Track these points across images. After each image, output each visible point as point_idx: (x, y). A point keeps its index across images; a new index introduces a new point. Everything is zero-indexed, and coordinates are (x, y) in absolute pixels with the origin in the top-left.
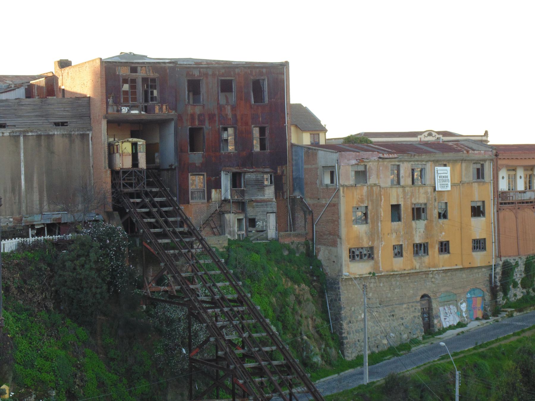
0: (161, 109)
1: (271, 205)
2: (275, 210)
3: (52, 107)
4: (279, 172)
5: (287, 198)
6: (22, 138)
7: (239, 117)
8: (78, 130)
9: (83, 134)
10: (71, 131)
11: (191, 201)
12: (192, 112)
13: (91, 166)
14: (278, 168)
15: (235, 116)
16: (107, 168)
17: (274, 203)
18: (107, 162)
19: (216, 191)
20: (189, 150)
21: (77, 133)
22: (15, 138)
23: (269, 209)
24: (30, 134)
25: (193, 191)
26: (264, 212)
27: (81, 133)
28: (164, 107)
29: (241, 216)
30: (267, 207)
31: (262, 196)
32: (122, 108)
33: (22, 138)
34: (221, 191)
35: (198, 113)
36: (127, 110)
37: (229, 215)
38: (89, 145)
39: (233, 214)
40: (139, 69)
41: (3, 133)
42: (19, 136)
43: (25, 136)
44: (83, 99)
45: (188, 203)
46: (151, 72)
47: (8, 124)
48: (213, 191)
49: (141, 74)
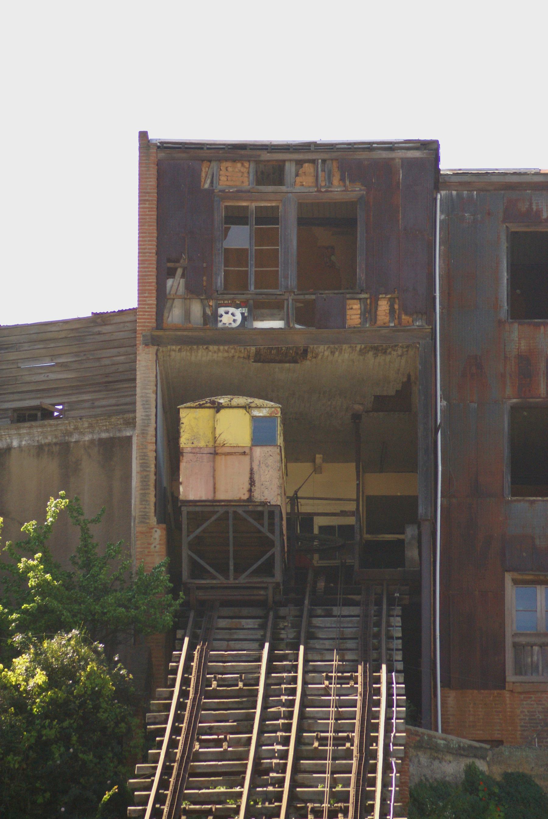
3: (12, 356)
8: (91, 426)
10: (70, 434)
11: (510, 677)
12: (523, 345)
16: (153, 520)
18: (152, 499)
20: (507, 490)
21: (87, 438)
25: (522, 640)
27: (104, 435)
28: (383, 306)
32: (221, 310)
36: (239, 318)
38: (127, 478)
40: (290, 169)
44: (118, 319)
45: (501, 683)
46: (336, 181)
49: (298, 188)
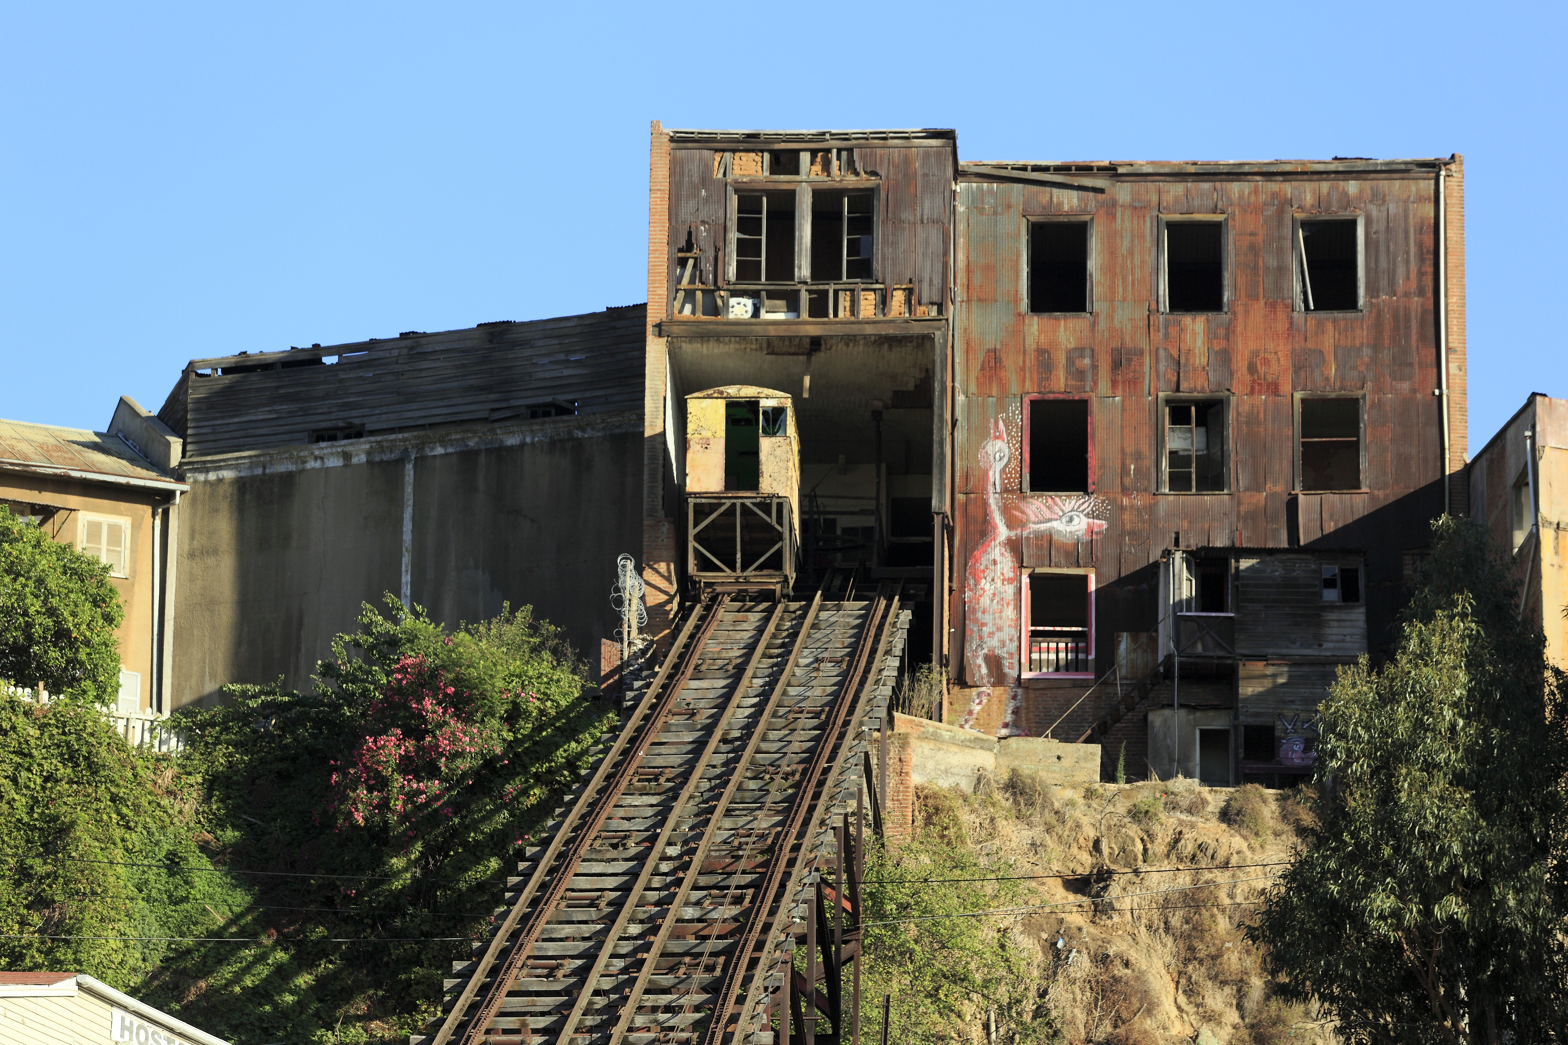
0: (884, 302)
3: (527, 352)
6: (409, 468)
7: (1240, 365)
16: (661, 513)
19: (1135, 639)
22: (386, 472)
24: (439, 451)
29: (1218, 722)
33: (409, 468)
34: (1155, 641)
37: (1167, 712)
38: (639, 474)
39: (1183, 713)
41: (347, 456)
42: (401, 461)
43: (421, 462)
47: (368, 427)
48: (1124, 644)
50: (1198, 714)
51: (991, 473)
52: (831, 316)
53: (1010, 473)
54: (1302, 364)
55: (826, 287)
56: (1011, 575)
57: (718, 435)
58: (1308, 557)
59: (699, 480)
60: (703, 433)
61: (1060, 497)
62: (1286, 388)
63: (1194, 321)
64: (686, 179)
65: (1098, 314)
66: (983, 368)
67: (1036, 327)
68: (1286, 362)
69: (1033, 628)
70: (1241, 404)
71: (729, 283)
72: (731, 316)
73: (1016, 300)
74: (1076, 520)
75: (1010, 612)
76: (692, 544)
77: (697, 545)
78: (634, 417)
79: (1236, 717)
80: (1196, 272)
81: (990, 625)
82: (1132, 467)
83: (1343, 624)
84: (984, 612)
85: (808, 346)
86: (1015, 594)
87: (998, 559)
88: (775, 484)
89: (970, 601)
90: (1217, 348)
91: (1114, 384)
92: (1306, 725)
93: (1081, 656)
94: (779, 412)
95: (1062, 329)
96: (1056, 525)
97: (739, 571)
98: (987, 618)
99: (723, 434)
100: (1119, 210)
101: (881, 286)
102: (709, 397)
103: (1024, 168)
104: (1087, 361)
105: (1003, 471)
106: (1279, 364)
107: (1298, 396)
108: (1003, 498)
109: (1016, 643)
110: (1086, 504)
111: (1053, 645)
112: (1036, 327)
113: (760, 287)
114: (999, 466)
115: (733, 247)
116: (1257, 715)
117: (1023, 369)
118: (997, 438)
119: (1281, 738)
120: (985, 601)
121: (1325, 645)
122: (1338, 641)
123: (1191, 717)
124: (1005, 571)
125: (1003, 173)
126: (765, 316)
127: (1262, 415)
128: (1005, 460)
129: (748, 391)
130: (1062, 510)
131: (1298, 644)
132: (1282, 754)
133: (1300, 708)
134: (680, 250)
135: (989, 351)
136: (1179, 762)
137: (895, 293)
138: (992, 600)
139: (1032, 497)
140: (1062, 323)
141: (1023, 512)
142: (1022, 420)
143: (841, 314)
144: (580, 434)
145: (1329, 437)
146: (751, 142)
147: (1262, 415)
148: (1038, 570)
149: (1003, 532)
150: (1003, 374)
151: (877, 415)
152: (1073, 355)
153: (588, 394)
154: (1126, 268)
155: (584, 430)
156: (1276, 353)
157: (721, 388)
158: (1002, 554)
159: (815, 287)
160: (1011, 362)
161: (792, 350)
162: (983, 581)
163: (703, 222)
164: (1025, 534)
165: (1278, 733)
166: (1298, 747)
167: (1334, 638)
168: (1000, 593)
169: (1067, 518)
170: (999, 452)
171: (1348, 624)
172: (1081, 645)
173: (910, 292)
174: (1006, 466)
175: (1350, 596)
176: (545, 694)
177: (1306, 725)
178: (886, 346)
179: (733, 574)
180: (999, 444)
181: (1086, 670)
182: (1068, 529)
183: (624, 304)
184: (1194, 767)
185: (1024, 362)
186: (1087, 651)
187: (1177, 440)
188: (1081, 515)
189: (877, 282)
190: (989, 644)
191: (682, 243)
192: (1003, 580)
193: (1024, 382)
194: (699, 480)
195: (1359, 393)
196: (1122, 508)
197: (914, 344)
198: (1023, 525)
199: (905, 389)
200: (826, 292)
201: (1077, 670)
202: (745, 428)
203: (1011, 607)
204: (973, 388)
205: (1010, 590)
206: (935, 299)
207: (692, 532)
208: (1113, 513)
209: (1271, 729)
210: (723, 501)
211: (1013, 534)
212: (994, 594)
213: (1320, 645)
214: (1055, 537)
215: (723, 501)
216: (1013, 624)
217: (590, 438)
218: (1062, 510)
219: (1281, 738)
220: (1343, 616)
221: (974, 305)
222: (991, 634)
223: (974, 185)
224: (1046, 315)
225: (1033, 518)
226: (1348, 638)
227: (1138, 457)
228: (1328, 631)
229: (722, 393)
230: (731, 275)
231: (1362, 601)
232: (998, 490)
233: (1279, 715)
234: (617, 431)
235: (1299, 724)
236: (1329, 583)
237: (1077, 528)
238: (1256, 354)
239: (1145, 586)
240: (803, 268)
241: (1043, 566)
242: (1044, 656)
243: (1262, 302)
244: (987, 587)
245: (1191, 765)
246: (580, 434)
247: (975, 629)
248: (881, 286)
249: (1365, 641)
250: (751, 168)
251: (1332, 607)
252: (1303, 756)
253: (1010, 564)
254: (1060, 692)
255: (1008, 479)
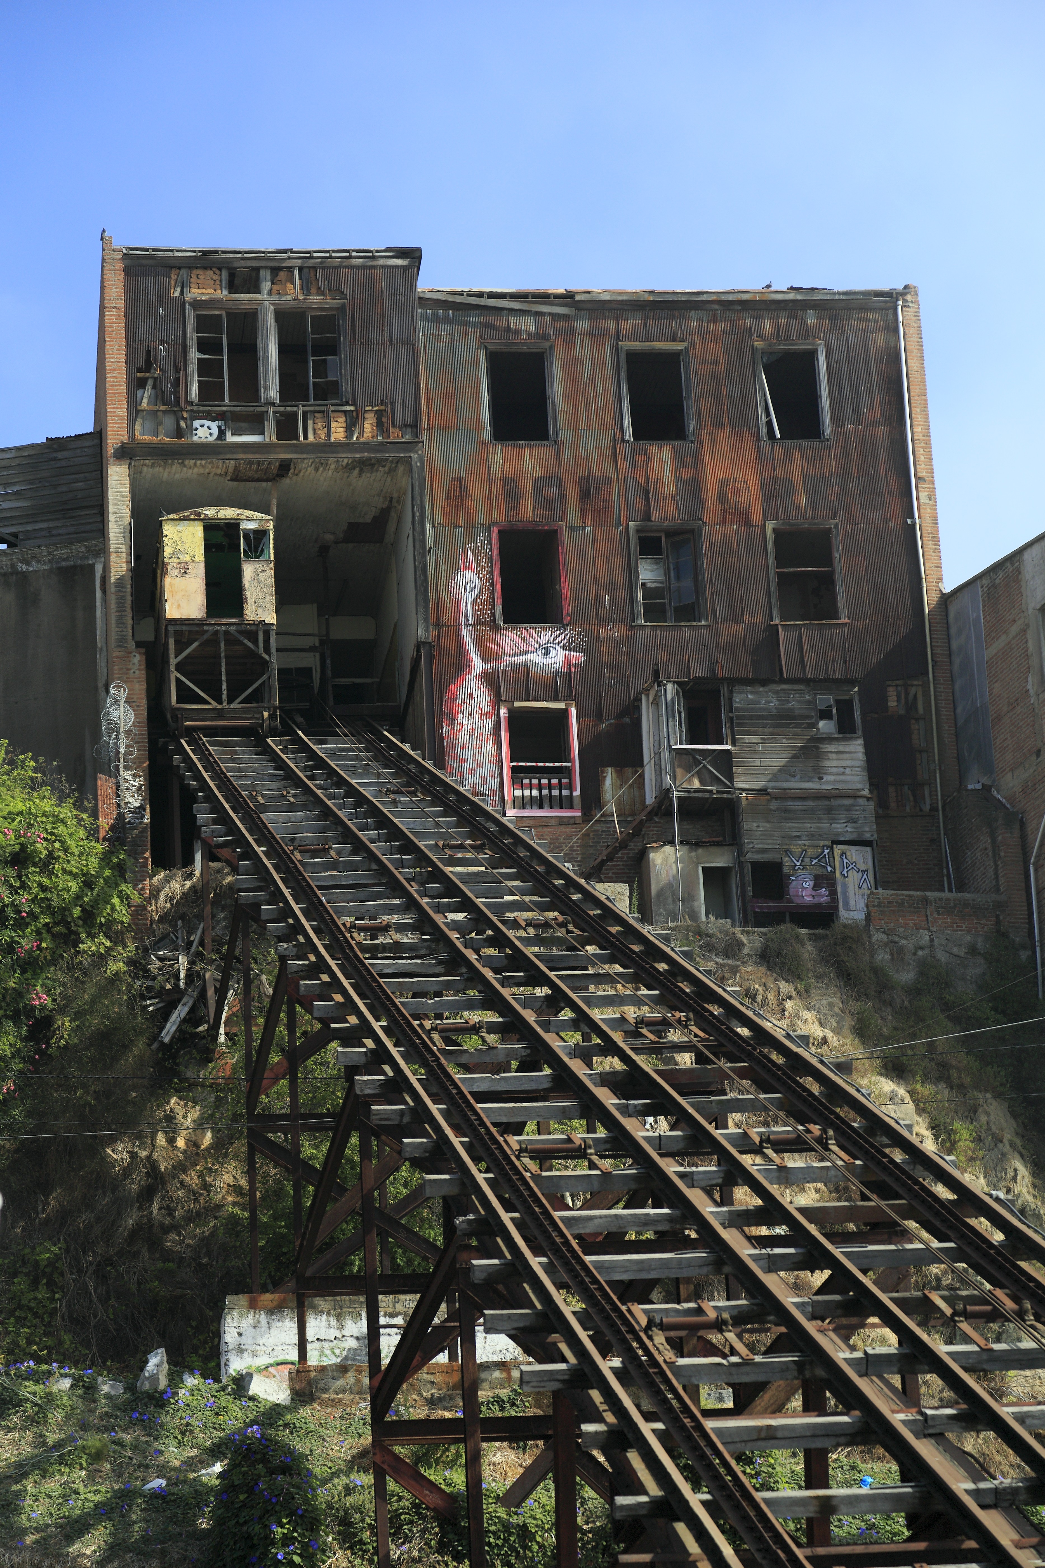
1: (848, 809)
2: (869, 831)
4: (892, 703)
5: (934, 809)
9: (74, 567)
13: (100, 684)
14: (892, 692)
15: (693, 488)
17: (861, 801)
19: (620, 774)
23: (843, 828)
26: (821, 837)
29: (721, 859)
30: (832, 821)
31: (809, 780)
32: (197, 423)
34: (642, 776)
35: (538, 474)
36: (215, 431)
48: (609, 779)
50: (700, 851)
51: (463, 605)
52: (302, 438)
53: (482, 604)
54: (774, 492)
55: (295, 409)
56: (488, 709)
57: (197, 559)
58: (802, 687)
59: (179, 606)
60: (181, 557)
61: (535, 629)
62: (757, 517)
63: (660, 448)
64: (142, 297)
65: (563, 443)
66: (448, 498)
67: (500, 455)
68: (755, 491)
69: (514, 764)
70: (715, 532)
71: (191, 403)
72: (195, 439)
73: (479, 428)
74: (553, 653)
75: (490, 747)
76: (174, 675)
77: (179, 675)
78: (83, 549)
79: (741, 853)
80: (658, 399)
81: (470, 761)
82: (607, 598)
83: (842, 756)
84: (463, 748)
85: (275, 472)
86: (494, 728)
87: (474, 692)
88: (260, 611)
89: (449, 737)
90: (685, 477)
91: (583, 513)
92: (815, 861)
93: (565, 793)
94: (261, 534)
95: (527, 457)
96: (532, 657)
97: (225, 704)
98: (467, 754)
99: (203, 559)
100: (578, 338)
101: (352, 408)
102: (186, 519)
103: (480, 295)
104: (555, 490)
105: (474, 602)
106: (750, 493)
107: (770, 526)
108: (476, 630)
109: (497, 780)
110: (562, 636)
111: (535, 781)
112: (500, 457)
113: (225, 409)
114: (470, 598)
115: (193, 368)
116: (764, 851)
117: (490, 498)
118: (466, 568)
119: (788, 876)
120: (464, 737)
121: (826, 778)
122: (837, 774)
123: (693, 854)
124: (483, 705)
125: (459, 299)
126: (231, 438)
127: (735, 545)
128: (477, 591)
129: (228, 513)
130: (538, 642)
131: (798, 776)
132: (792, 891)
133: (807, 843)
134: (139, 370)
135: (453, 479)
136: (683, 901)
137: (366, 415)
138: (471, 736)
139: (506, 629)
140: (527, 451)
141: (498, 644)
142: (491, 550)
143: (311, 437)
144: (24, 568)
145: (805, 568)
146: (207, 261)
147: (735, 545)
148: (517, 704)
149: (478, 665)
150: (470, 503)
151: (324, 550)
152: (540, 484)
153: (29, 527)
154: (586, 398)
155: (28, 563)
156: (745, 482)
157: (198, 510)
158: (479, 688)
159: (282, 409)
160: (477, 491)
161: (256, 476)
162: (461, 716)
163: (162, 342)
164: (501, 666)
165: (786, 870)
166: (808, 884)
167: (834, 770)
168: (479, 728)
169: (545, 651)
170: (470, 585)
171: (847, 756)
172: (564, 781)
173: (379, 414)
174: (478, 597)
175: (846, 728)
176: (52, 834)
177: (815, 861)
178: (357, 471)
179: (219, 707)
180: (469, 575)
181: (571, 807)
182: (545, 661)
183: (66, 435)
184: (700, 907)
185: (490, 491)
186: (571, 787)
187: (648, 573)
188: (558, 648)
189: (347, 404)
190: (470, 780)
191: (141, 362)
192: (481, 715)
193: (491, 510)
194: (179, 606)
195: (832, 523)
196: (599, 640)
197: (387, 469)
198: (499, 657)
199: (361, 520)
200: (295, 414)
201: (561, 808)
202: (224, 551)
203: (491, 743)
204: (439, 518)
205: (489, 724)
206: (409, 421)
207: (173, 661)
208: (590, 646)
209: (778, 866)
210: (205, 628)
211: (488, 667)
212: (472, 729)
213: (821, 778)
214: (533, 670)
215: (205, 628)
216: (493, 760)
217: (36, 571)
218: (538, 642)
219: (788, 876)
220: (841, 748)
221: (434, 433)
222: (472, 771)
223: (429, 311)
224: (510, 442)
225: (508, 650)
226: (848, 771)
227: (612, 588)
228: (827, 763)
229: (199, 514)
230: (194, 395)
231: (859, 732)
232: (471, 622)
233: (787, 851)
234: (64, 564)
235: (807, 860)
236: (825, 714)
237: (554, 660)
238: (725, 482)
239: (627, 720)
240: (272, 389)
241: (521, 700)
242: (527, 793)
243: (728, 430)
244: (465, 721)
245: (696, 904)
246: (24, 568)
247: (455, 765)
248: (352, 408)
249: (865, 774)
250: (206, 290)
251: (830, 739)
252: (814, 893)
253: (488, 698)
254: (546, 830)
255: (481, 610)
